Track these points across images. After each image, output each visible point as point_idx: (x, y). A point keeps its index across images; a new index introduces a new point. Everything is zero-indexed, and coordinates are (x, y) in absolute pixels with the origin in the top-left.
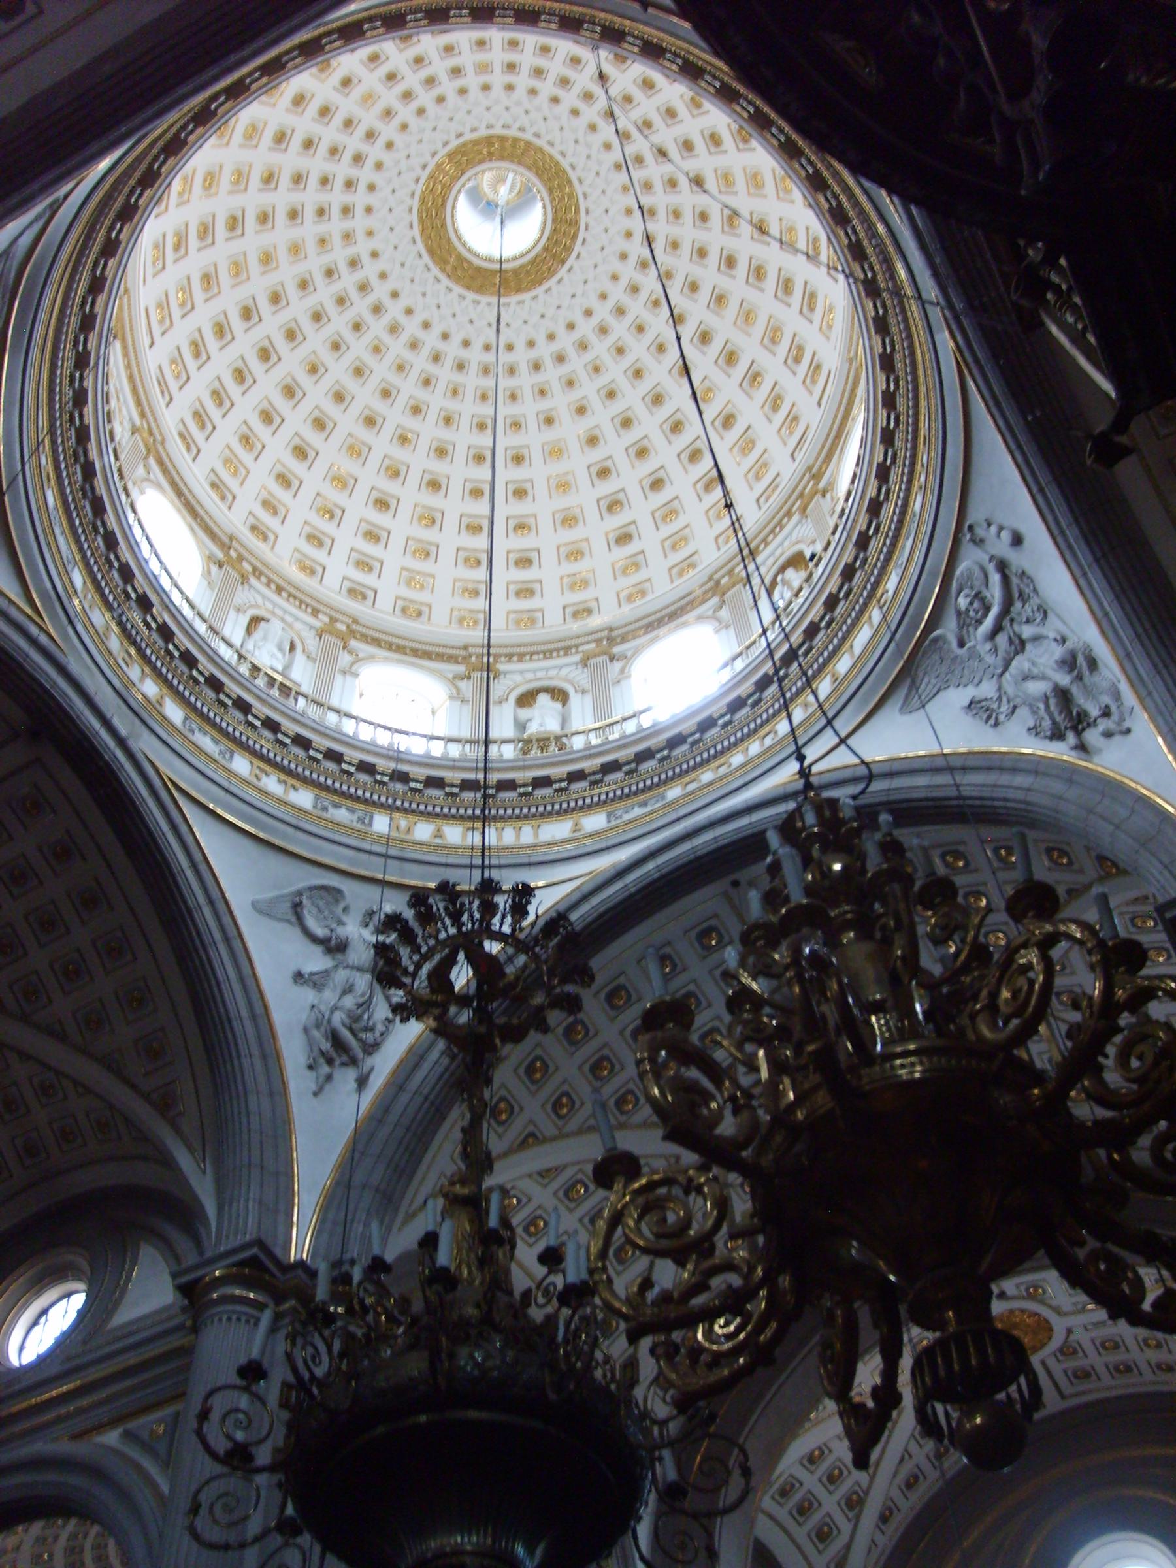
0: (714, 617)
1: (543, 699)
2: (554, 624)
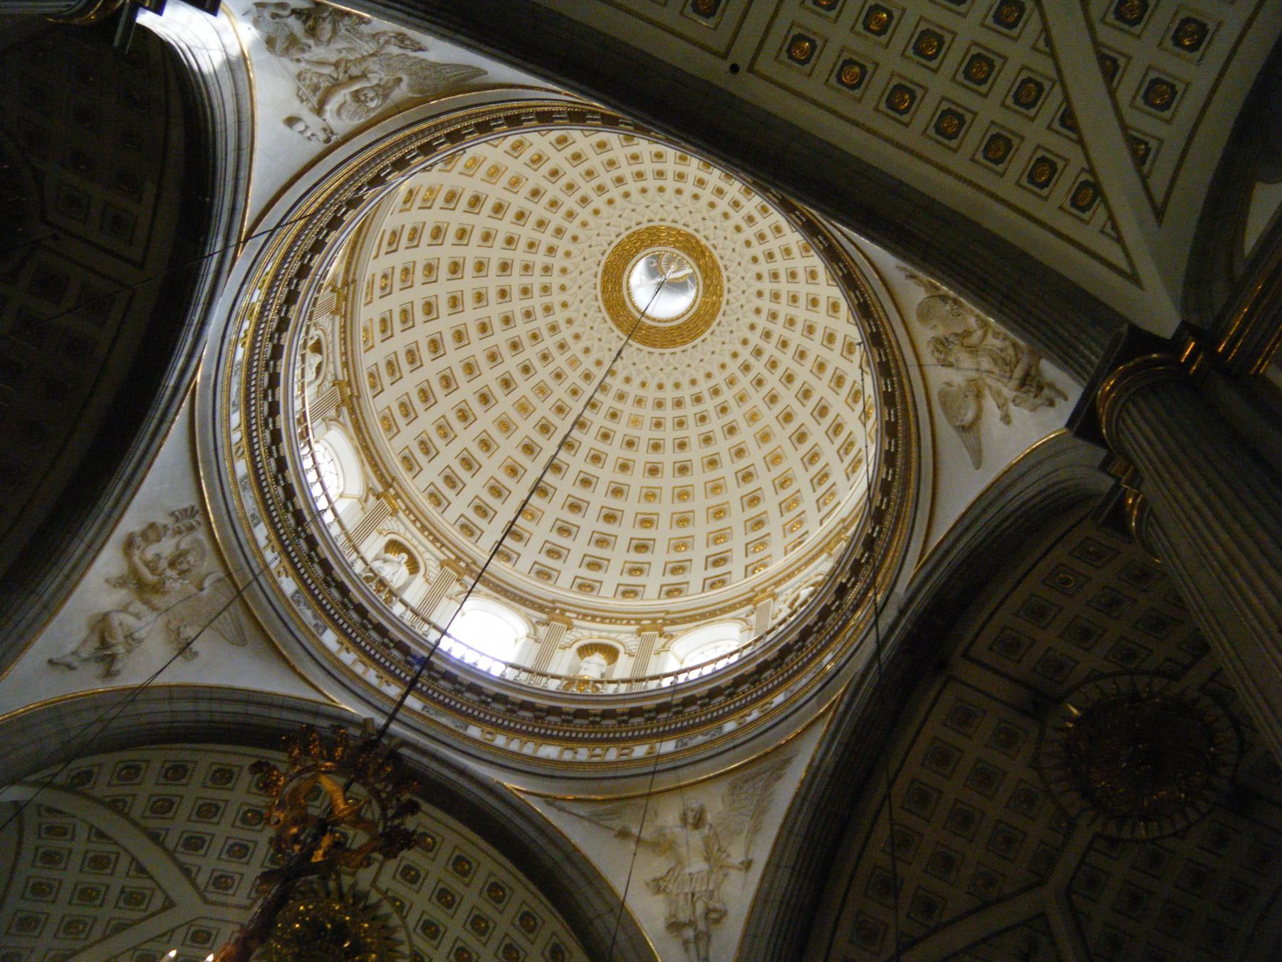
0: (535, 625)
1: (405, 556)
2: (447, 522)
